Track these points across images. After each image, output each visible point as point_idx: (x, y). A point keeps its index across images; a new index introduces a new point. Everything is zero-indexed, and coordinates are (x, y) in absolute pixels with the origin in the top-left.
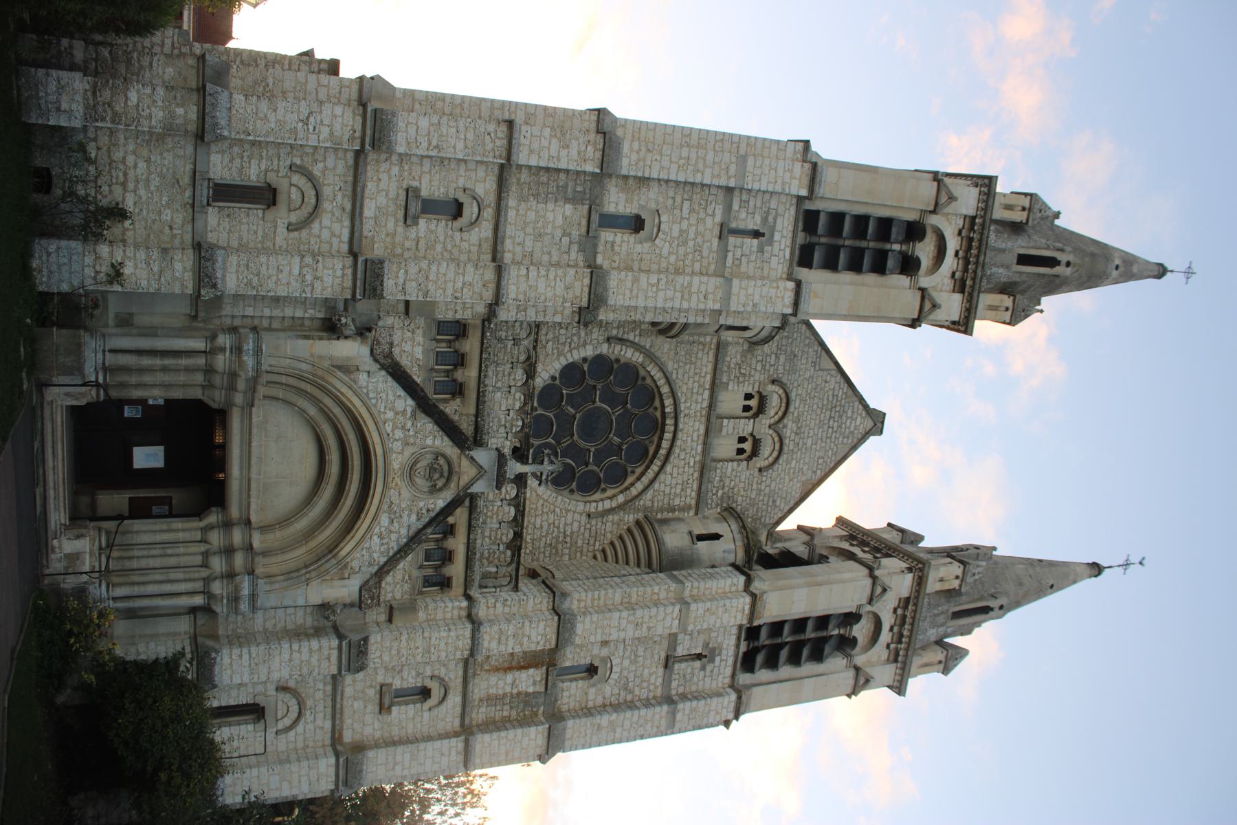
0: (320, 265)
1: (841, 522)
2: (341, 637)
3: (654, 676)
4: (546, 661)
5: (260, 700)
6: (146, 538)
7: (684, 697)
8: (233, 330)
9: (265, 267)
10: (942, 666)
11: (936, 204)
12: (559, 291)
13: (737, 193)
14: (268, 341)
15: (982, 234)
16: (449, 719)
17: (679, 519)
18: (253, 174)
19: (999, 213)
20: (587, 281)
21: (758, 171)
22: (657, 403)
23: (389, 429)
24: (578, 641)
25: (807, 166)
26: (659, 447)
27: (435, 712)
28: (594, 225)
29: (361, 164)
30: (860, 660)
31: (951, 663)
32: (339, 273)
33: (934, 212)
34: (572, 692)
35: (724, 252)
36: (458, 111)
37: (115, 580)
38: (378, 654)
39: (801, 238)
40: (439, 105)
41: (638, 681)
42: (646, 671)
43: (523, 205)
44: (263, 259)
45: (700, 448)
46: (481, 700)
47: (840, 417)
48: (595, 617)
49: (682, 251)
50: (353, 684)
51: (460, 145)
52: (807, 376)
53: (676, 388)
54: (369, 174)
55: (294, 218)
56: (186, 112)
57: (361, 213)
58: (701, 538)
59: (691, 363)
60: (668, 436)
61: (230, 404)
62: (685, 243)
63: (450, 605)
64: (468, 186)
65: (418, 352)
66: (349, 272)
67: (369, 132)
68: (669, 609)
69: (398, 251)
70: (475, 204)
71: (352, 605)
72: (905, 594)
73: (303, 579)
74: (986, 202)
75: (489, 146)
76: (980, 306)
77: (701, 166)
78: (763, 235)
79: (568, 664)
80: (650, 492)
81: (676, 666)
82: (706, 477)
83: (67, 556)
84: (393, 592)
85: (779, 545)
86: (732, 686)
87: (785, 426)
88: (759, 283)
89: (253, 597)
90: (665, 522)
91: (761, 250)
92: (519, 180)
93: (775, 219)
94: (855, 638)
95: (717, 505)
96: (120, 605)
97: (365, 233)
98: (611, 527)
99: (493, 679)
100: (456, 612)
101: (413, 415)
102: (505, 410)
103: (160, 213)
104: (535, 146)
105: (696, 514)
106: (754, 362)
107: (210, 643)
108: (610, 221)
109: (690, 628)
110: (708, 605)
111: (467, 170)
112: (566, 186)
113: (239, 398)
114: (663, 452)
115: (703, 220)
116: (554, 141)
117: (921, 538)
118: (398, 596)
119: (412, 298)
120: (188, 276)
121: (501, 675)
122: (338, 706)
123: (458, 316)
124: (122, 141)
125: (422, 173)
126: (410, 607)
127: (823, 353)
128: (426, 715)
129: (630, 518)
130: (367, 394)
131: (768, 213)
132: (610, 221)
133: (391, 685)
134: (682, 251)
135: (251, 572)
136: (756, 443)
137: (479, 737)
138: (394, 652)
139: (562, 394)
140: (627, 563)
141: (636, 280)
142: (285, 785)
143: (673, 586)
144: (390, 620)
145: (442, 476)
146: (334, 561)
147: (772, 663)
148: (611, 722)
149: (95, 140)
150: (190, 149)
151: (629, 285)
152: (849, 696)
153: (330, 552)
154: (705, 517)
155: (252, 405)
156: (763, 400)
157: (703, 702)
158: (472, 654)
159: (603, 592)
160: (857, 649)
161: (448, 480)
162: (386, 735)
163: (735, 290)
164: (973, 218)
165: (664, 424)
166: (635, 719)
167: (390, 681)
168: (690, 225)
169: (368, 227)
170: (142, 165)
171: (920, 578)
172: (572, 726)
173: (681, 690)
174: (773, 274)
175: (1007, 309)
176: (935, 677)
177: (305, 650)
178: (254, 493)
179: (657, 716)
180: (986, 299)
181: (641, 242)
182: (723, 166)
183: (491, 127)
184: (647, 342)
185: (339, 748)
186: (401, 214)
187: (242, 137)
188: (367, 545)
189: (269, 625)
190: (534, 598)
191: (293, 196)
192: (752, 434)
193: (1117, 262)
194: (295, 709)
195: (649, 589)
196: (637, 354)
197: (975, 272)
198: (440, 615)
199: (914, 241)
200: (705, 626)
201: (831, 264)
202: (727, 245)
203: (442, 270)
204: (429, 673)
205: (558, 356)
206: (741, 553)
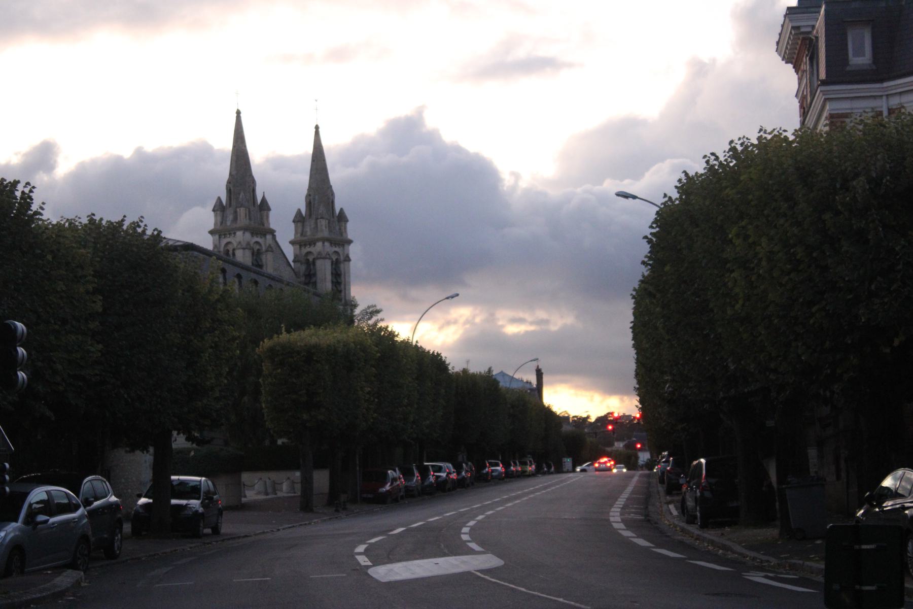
94: (337, 259)
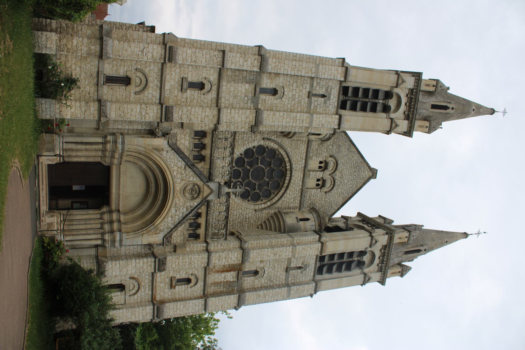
0: (148, 108)
1: (359, 214)
2: (155, 257)
3: (282, 275)
4: (238, 269)
5: (123, 283)
6: (78, 217)
7: (294, 284)
8: (113, 134)
9: (126, 109)
10: (400, 274)
11: (397, 84)
12: (243, 119)
13: (315, 79)
14: (127, 139)
15: (416, 96)
16: (199, 291)
17: (292, 212)
18: (121, 73)
19: (423, 88)
20: (254, 115)
21: (324, 71)
22: (283, 165)
23: (175, 174)
24: (251, 260)
25: (344, 68)
26: (284, 183)
27: (193, 288)
28: (258, 92)
29: (164, 68)
30: (366, 270)
31: (404, 273)
32: (156, 111)
33: (396, 87)
34: (248, 281)
35: (310, 103)
36: (203, 47)
37: (66, 233)
38: (170, 264)
39: (342, 97)
40: (195, 44)
41: (275, 277)
42: (278, 274)
43: (229, 84)
44: (126, 106)
45: (301, 183)
46: (211, 284)
47: (359, 171)
48: (258, 251)
49: (293, 103)
50: (160, 277)
51: (204, 60)
52: (345, 154)
53: (291, 159)
54: (167, 72)
55: (137, 89)
56: (95, 48)
57: (164, 88)
58: (301, 220)
59: (297, 148)
60: (288, 178)
61: (112, 163)
62: (294, 100)
63: (199, 245)
64: (206, 77)
65: (187, 143)
66: (160, 111)
67: (167, 55)
68: (288, 248)
69: (179, 103)
70: (210, 84)
71: (160, 245)
72: (385, 243)
73: (141, 234)
74: (418, 83)
75: (215, 61)
76: (416, 126)
77: (300, 69)
78: (326, 96)
79: (247, 270)
80: (280, 202)
81: (291, 272)
82: (303, 194)
83: (48, 224)
84: (176, 240)
85: (334, 223)
86: (313, 280)
87: (336, 175)
88: (324, 116)
89: (121, 241)
90: (286, 213)
91: (325, 102)
92: (227, 74)
93: (331, 90)
94: (364, 262)
95: (308, 207)
96: (68, 243)
97: (166, 95)
98: (265, 215)
99: (217, 275)
100: (202, 248)
101: (185, 168)
102: (222, 166)
103: (85, 88)
104: (234, 61)
105: (300, 210)
106: (323, 148)
107: (104, 259)
108: (264, 91)
109: (296, 256)
110: (304, 246)
111: (206, 70)
112: (246, 77)
113: (116, 161)
114: (286, 185)
115: (302, 91)
116: (241, 59)
117: (393, 221)
118: (178, 241)
119: (184, 122)
120: (96, 113)
121: (220, 274)
122: (154, 285)
123: (203, 129)
124: (70, 59)
125: (189, 71)
126: (184, 246)
127: (352, 145)
128: (189, 289)
129: (272, 211)
130: (167, 160)
131: (328, 87)
132: (264, 91)
133: (175, 277)
134: (293, 103)
135: (120, 231)
136: (324, 181)
137: (211, 299)
138: (177, 264)
139: (245, 161)
140: (271, 230)
141: (274, 115)
142: (133, 316)
143: (290, 239)
144: (175, 251)
145: (196, 193)
146: (153, 227)
147: (330, 271)
148: (264, 294)
149: (60, 59)
150: (96, 62)
151: (272, 116)
152: (362, 285)
153: (152, 223)
154: (303, 212)
155: (121, 164)
156: (327, 164)
157: (301, 286)
158: (208, 265)
159: (261, 241)
160: (365, 266)
161: (199, 194)
162: (173, 297)
163: (315, 118)
164: (412, 90)
165: (286, 173)
166: (274, 292)
167: (175, 276)
168: (296, 92)
169: (167, 93)
170: (78, 69)
171: (391, 237)
172: (248, 296)
173: (293, 281)
174: (330, 112)
175: (427, 127)
176: (397, 278)
177: (141, 262)
178: (121, 199)
179: (283, 292)
180: (418, 123)
181: (276, 99)
182: (310, 69)
183: (216, 53)
184: (279, 140)
185: (155, 302)
186: (180, 88)
187: (117, 57)
188: (166, 220)
189: (127, 252)
190: (233, 243)
191: (137, 81)
192: (322, 178)
193: (474, 108)
194: (137, 286)
195: (280, 240)
196: (275, 145)
197: (413, 112)
198: (195, 249)
199: (388, 99)
200: (303, 255)
201: (353, 108)
202: (311, 100)
203: (197, 110)
204: (191, 273)
205: (243, 145)
206: (317, 227)
